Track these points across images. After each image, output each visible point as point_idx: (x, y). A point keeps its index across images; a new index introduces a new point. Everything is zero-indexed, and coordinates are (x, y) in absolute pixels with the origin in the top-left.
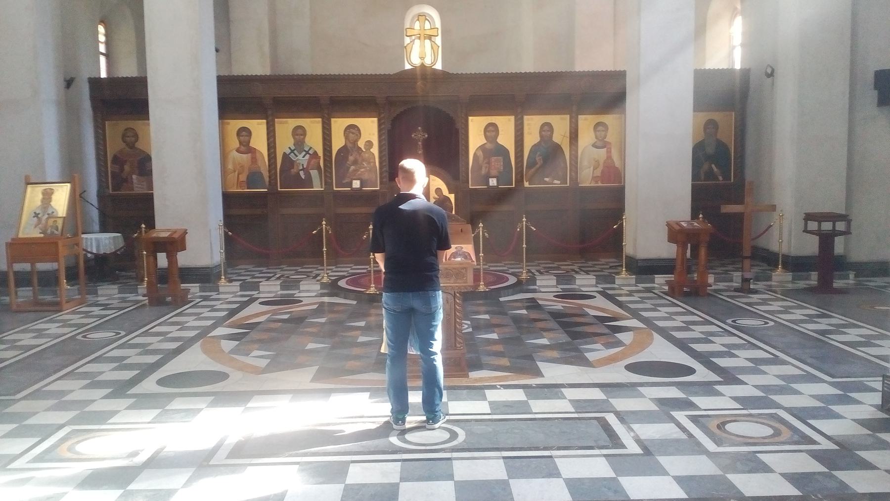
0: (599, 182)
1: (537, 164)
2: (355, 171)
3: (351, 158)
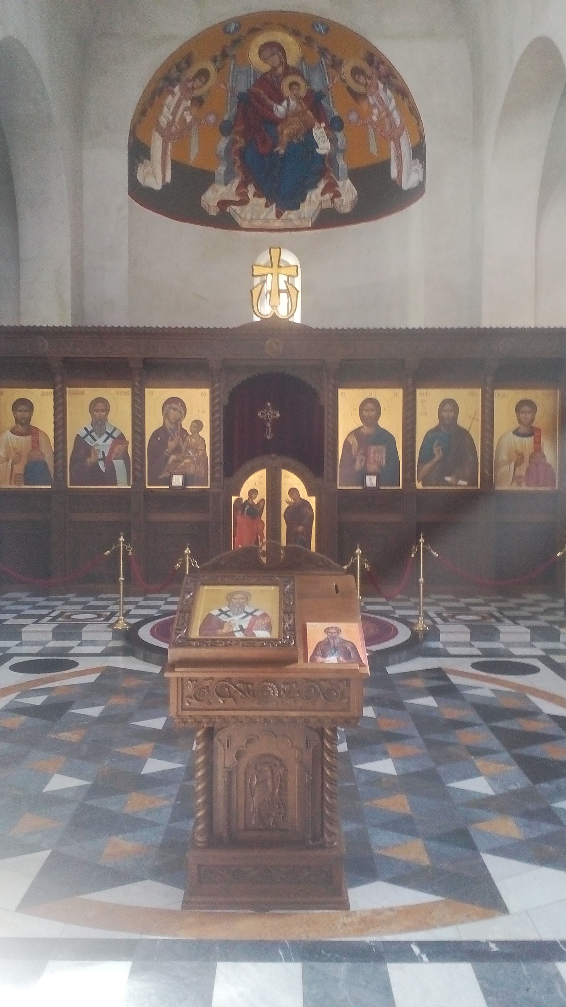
0: (523, 484)
2: (177, 461)
3: (171, 444)
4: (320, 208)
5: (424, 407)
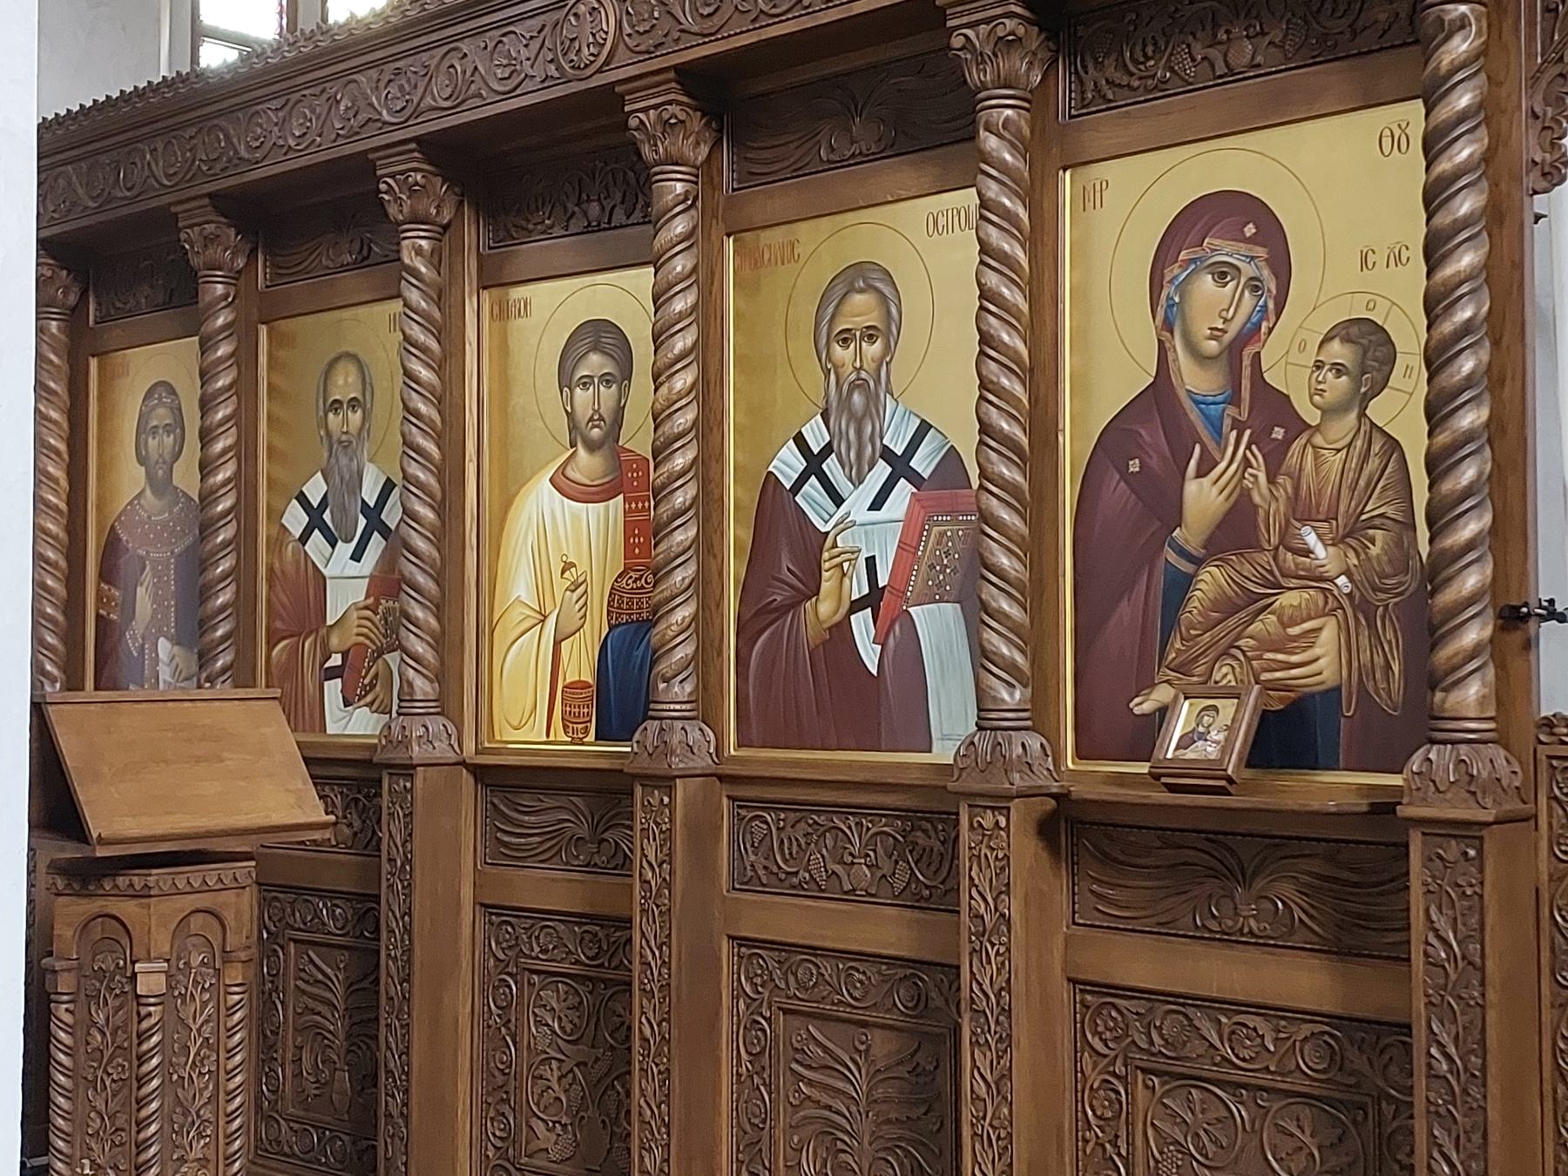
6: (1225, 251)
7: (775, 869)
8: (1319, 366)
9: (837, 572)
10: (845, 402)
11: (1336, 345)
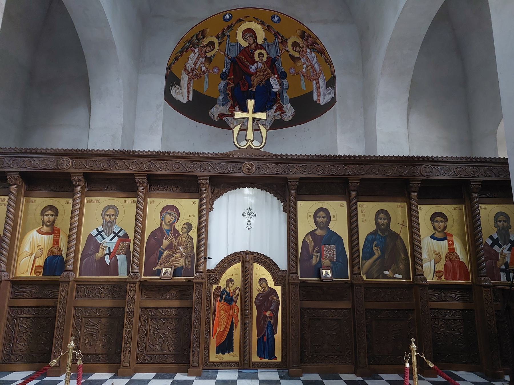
0: (443, 277)
1: (375, 254)
2: (170, 256)
3: (166, 242)
4: (274, 119)
5: (364, 216)
6: (171, 212)
7: (85, 295)
8: (183, 227)
9: (103, 249)
10: (107, 225)
11: (185, 225)
